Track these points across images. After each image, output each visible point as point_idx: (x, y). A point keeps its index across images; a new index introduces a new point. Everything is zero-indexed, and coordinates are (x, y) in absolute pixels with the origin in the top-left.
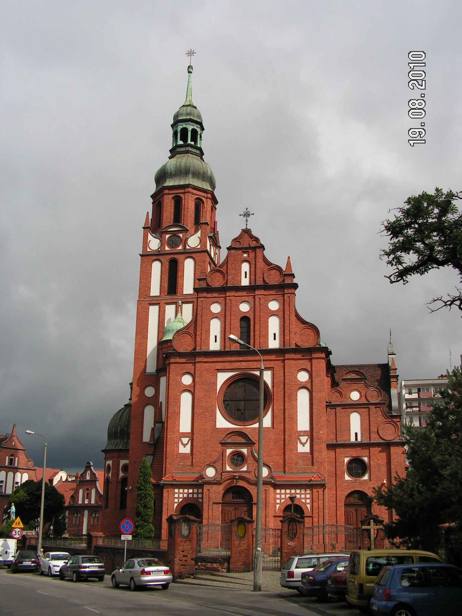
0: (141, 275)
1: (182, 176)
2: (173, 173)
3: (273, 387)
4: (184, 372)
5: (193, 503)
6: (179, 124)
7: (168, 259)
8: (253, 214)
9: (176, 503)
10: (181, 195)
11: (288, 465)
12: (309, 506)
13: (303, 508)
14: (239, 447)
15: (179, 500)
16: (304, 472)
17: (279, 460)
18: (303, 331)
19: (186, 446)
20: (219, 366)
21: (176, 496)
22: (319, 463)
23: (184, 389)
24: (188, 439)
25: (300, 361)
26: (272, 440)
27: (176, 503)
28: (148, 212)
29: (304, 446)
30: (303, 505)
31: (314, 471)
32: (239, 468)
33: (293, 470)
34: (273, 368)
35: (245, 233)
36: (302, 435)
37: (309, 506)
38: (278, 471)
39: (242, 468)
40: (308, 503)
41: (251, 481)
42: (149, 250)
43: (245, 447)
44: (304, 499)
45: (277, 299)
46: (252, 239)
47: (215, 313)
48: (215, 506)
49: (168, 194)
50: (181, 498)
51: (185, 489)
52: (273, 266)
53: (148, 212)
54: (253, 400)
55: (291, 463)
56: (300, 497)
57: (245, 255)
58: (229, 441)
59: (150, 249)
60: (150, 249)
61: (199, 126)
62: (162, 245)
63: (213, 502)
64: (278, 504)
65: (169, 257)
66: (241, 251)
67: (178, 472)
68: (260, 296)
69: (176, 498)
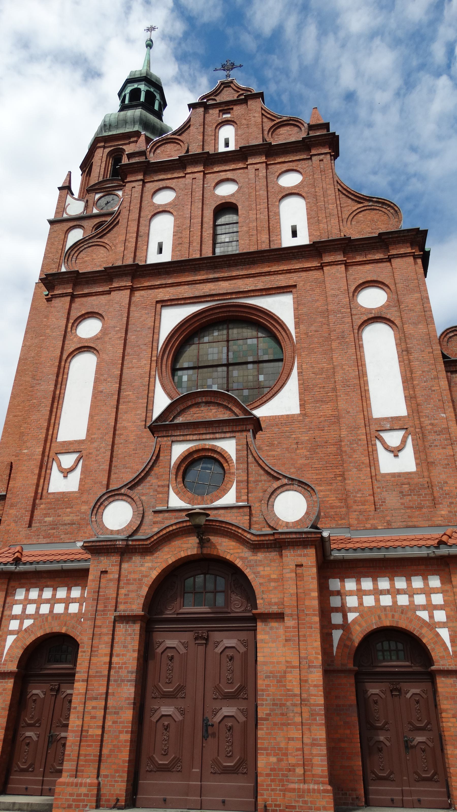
0: (48, 249)
1: (127, 126)
2: (113, 124)
3: (297, 325)
4: (83, 312)
5: (63, 631)
6: (129, 85)
7: (97, 222)
8: (241, 66)
9: (12, 633)
10: (124, 147)
11: (355, 507)
12: (444, 634)
13: (424, 641)
14: (208, 436)
15: (21, 624)
16: (408, 527)
17: (326, 496)
18: (360, 215)
19: (70, 476)
20: (163, 294)
21: (17, 610)
22: (451, 497)
23: (79, 346)
24: (74, 457)
25: (359, 267)
26: (302, 443)
27: (12, 633)
28: (70, 174)
29: (396, 456)
30: (425, 631)
31: (438, 521)
32: (209, 497)
33: (371, 522)
34: (295, 286)
35: (224, 87)
36: (388, 428)
37: (444, 634)
38: (328, 526)
39: (219, 498)
40: (443, 625)
41: (249, 536)
42: (65, 216)
43: (228, 435)
44: (424, 608)
45: (295, 168)
46: (239, 93)
47: (161, 205)
48: (121, 628)
49: (104, 147)
50: (29, 617)
51: (47, 586)
52: (285, 118)
53: (70, 174)
54: (247, 363)
55: (364, 503)
56: (412, 602)
57: (228, 116)
58: (180, 420)
59: (67, 214)
60: (67, 214)
61: (159, 92)
62: (86, 207)
63: (117, 614)
64: (337, 627)
65: (97, 221)
66: (218, 109)
67: (35, 542)
68: (259, 165)
69: (15, 617)
